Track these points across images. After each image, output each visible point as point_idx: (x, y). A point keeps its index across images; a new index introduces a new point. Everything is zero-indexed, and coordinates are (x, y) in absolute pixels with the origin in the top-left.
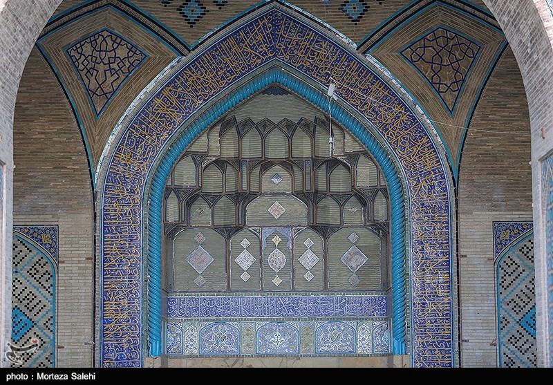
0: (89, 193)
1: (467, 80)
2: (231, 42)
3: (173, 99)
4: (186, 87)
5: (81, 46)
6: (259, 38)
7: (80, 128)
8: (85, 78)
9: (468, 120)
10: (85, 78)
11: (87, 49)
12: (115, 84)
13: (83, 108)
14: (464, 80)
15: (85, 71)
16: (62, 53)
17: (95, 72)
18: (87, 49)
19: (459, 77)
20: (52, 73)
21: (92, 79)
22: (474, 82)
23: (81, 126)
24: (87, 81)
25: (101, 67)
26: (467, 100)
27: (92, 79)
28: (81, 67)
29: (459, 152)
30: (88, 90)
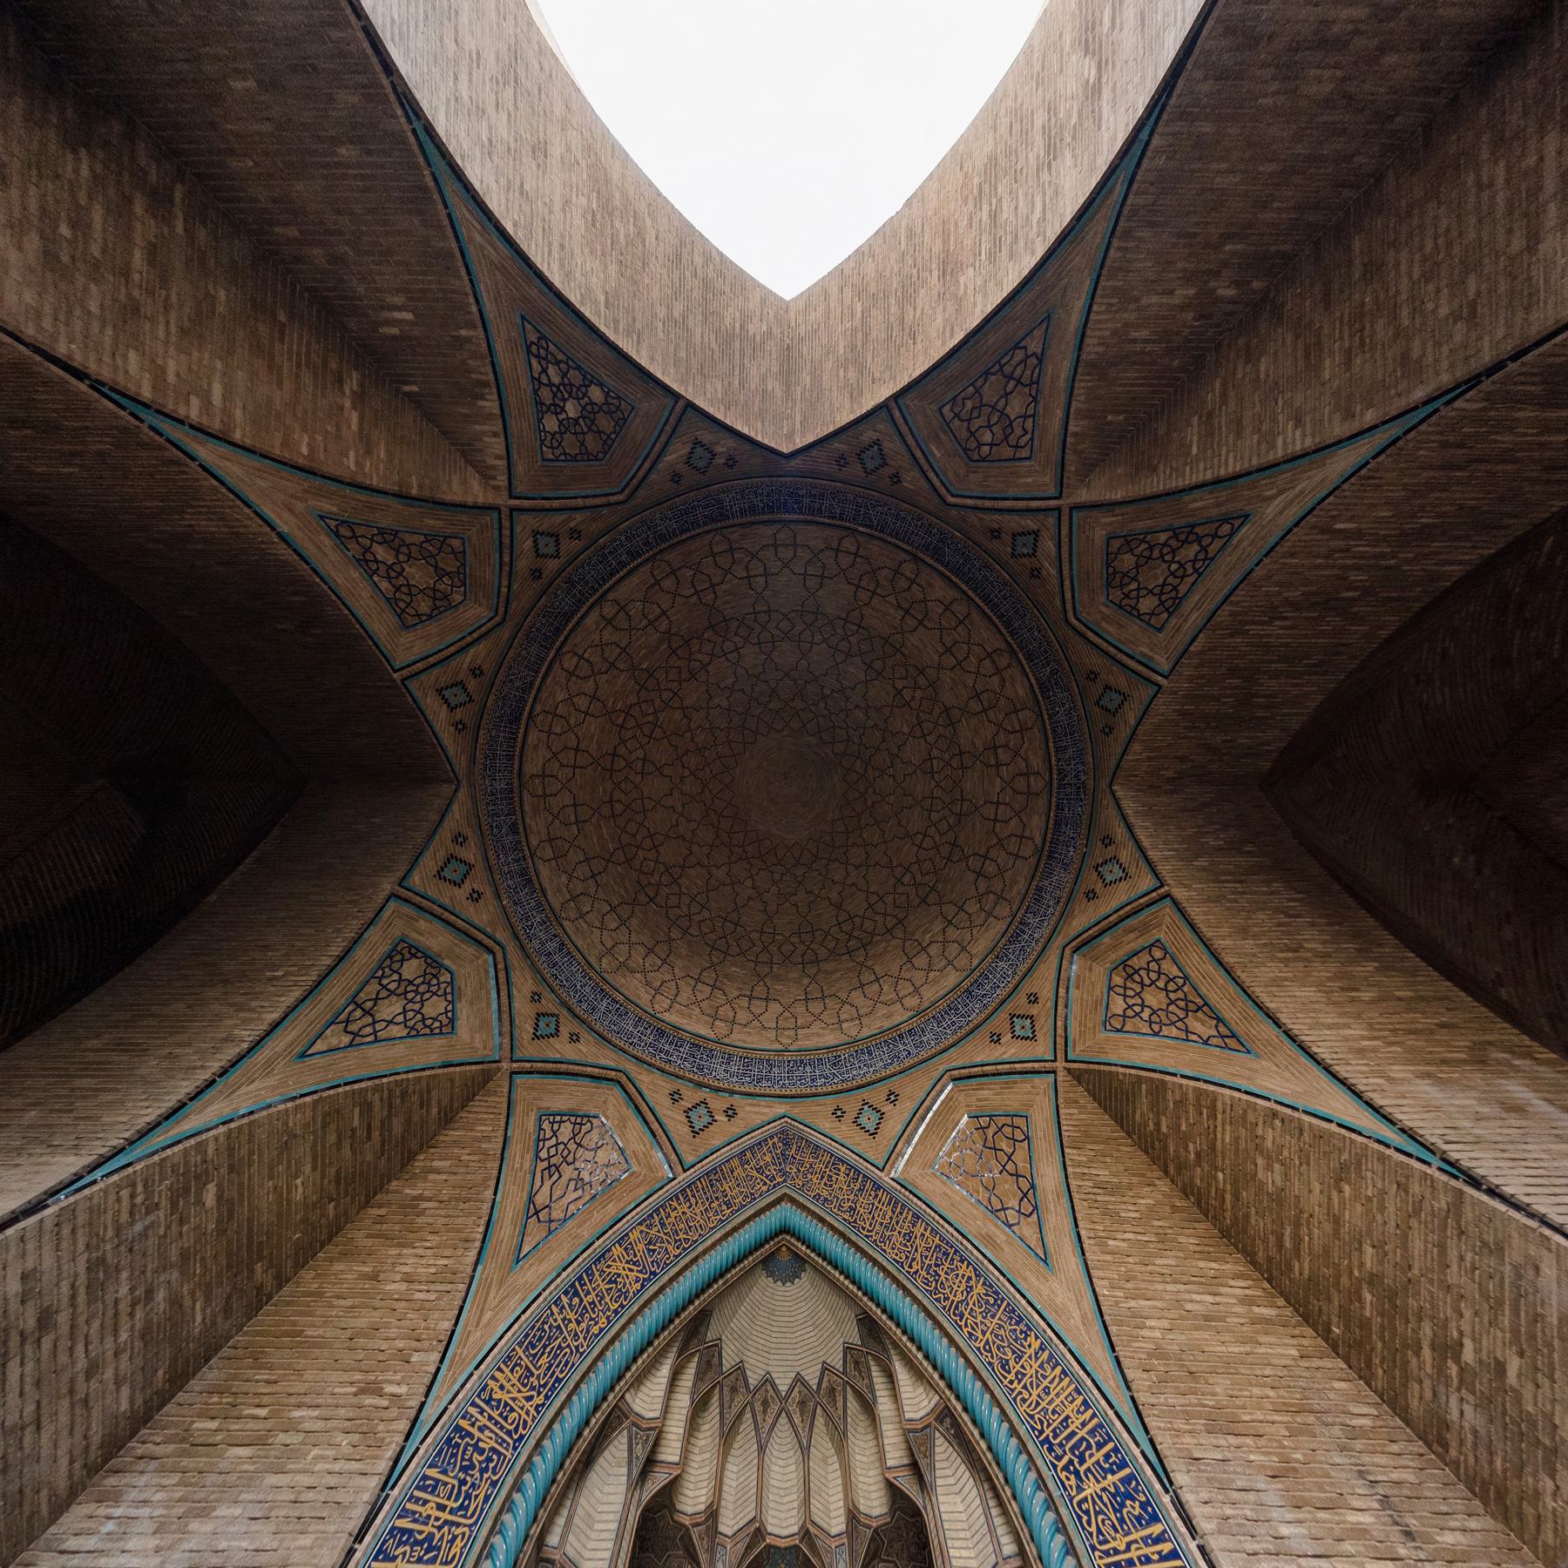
0: (351, 462)
1: (1036, 1181)
2: (736, 1162)
3: (641, 1246)
4: (663, 1225)
5: (561, 1122)
6: (768, 1158)
7: (474, 1270)
8: (538, 1175)
9: (1080, 1261)
10: (538, 1175)
11: (566, 1131)
12: (572, 1208)
13: (505, 1232)
14: (1033, 1186)
15: (545, 1164)
16: (533, 1117)
17: (556, 1176)
18: (566, 1131)
19: (1025, 1186)
20: (501, 1132)
21: (548, 1184)
22: (1049, 1177)
23: (480, 1268)
24: (538, 1183)
25: (568, 1172)
26: (1056, 1218)
27: (548, 1184)
28: (544, 1154)
29: (1109, 1355)
30: (531, 1200)
